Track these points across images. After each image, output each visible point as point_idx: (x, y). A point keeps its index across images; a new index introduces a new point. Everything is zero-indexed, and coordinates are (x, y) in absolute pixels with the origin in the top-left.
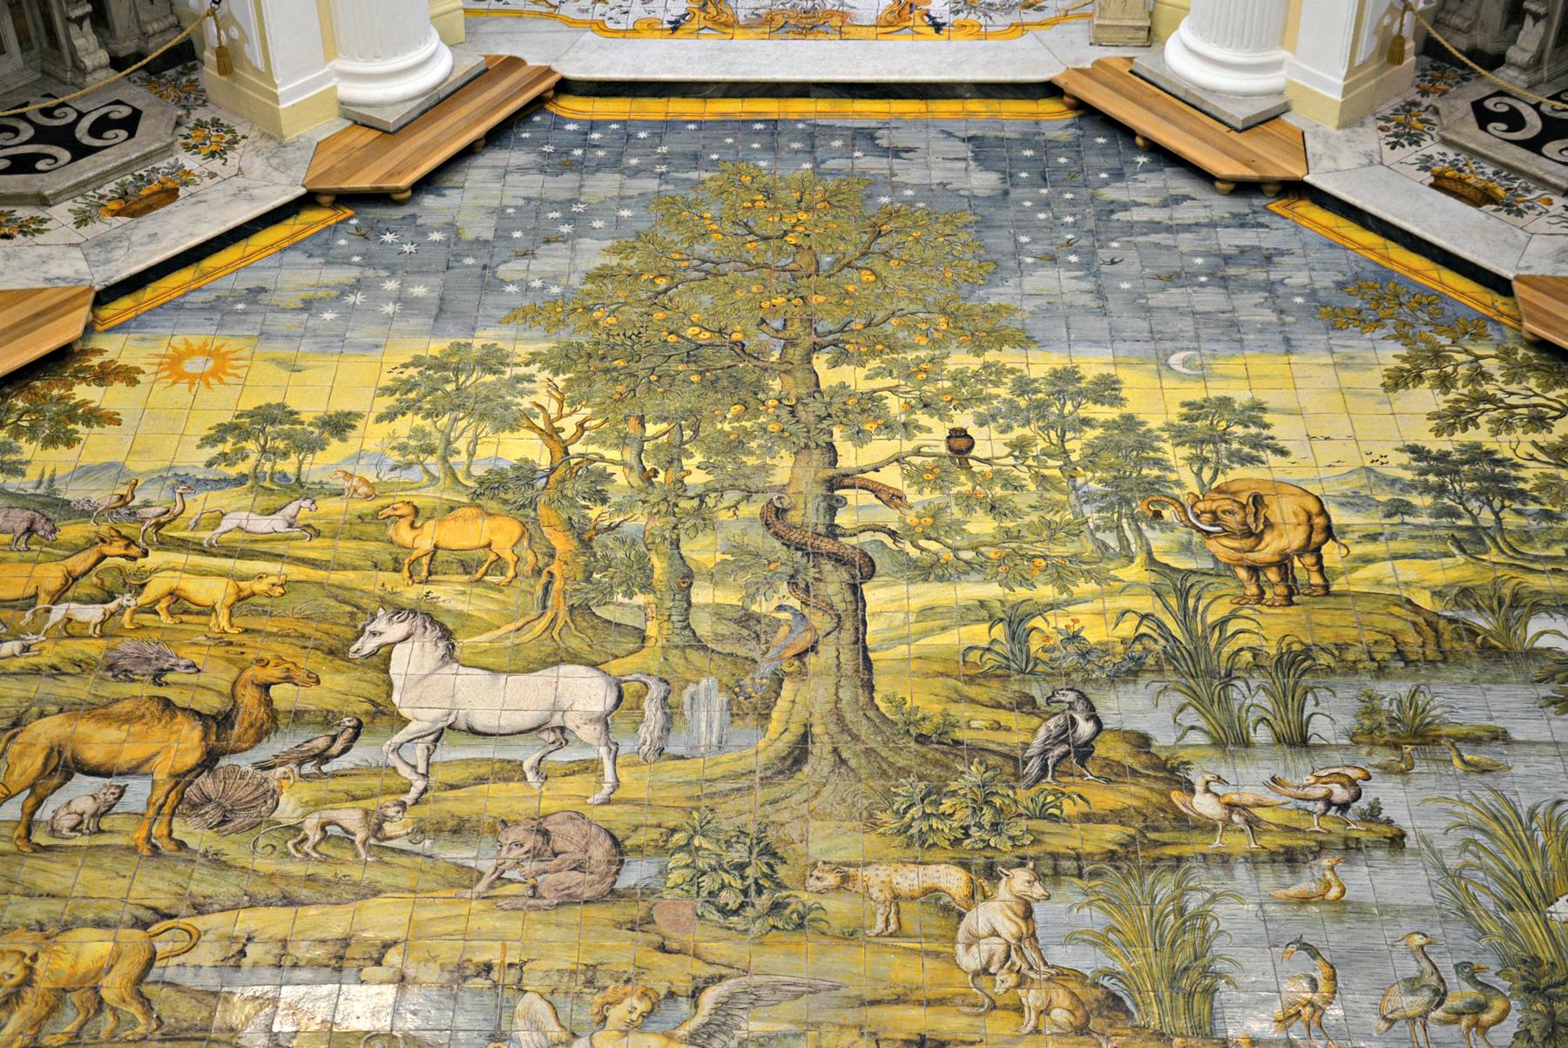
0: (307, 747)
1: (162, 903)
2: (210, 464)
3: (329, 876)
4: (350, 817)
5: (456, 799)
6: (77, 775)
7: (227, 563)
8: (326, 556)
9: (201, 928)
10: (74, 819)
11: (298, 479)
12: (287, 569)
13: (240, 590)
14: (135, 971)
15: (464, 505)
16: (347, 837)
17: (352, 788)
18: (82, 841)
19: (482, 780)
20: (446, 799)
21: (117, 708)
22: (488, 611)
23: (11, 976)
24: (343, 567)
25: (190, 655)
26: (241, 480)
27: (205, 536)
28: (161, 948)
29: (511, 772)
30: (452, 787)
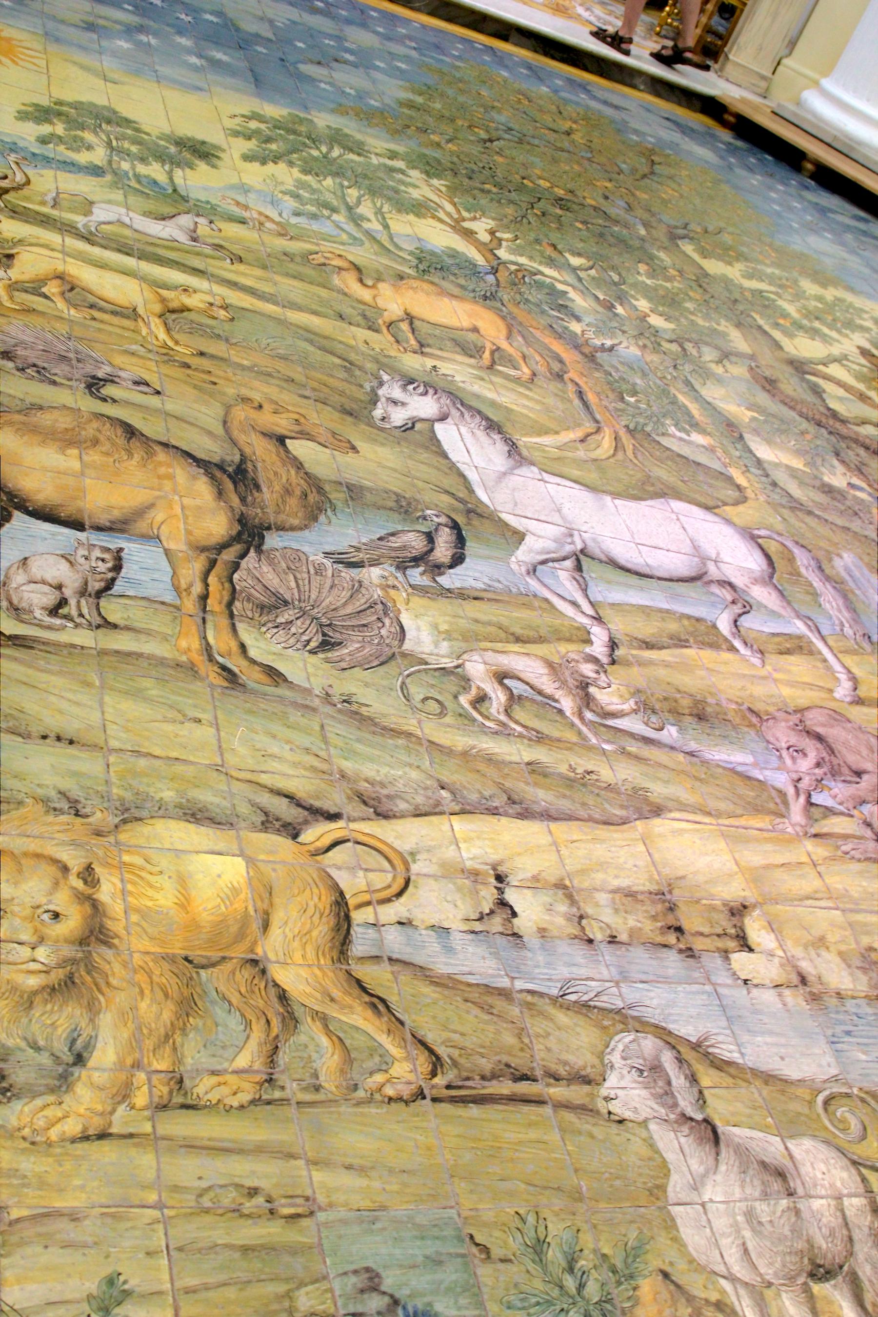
0: (396, 542)
1: (300, 784)
2: (43, 141)
3: (563, 769)
4: (529, 666)
5: (667, 665)
6: (17, 514)
7: (131, 262)
8: (266, 288)
9: (405, 846)
10: (51, 598)
11: (175, 190)
12: (217, 289)
13: (163, 300)
14: (322, 930)
15: (409, 277)
16: (546, 702)
17: (505, 622)
18: (83, 637)
19: (680, 642)
20: (650, 663)
21: (46, 419)
22: (531, 409)
23: (56, 916)
24: (300, 308)
25: (131, 368)
26: (96, 171)
27: (80, 221)
28: (353, 884)
29: (707, 637)
30: (649, 646)
